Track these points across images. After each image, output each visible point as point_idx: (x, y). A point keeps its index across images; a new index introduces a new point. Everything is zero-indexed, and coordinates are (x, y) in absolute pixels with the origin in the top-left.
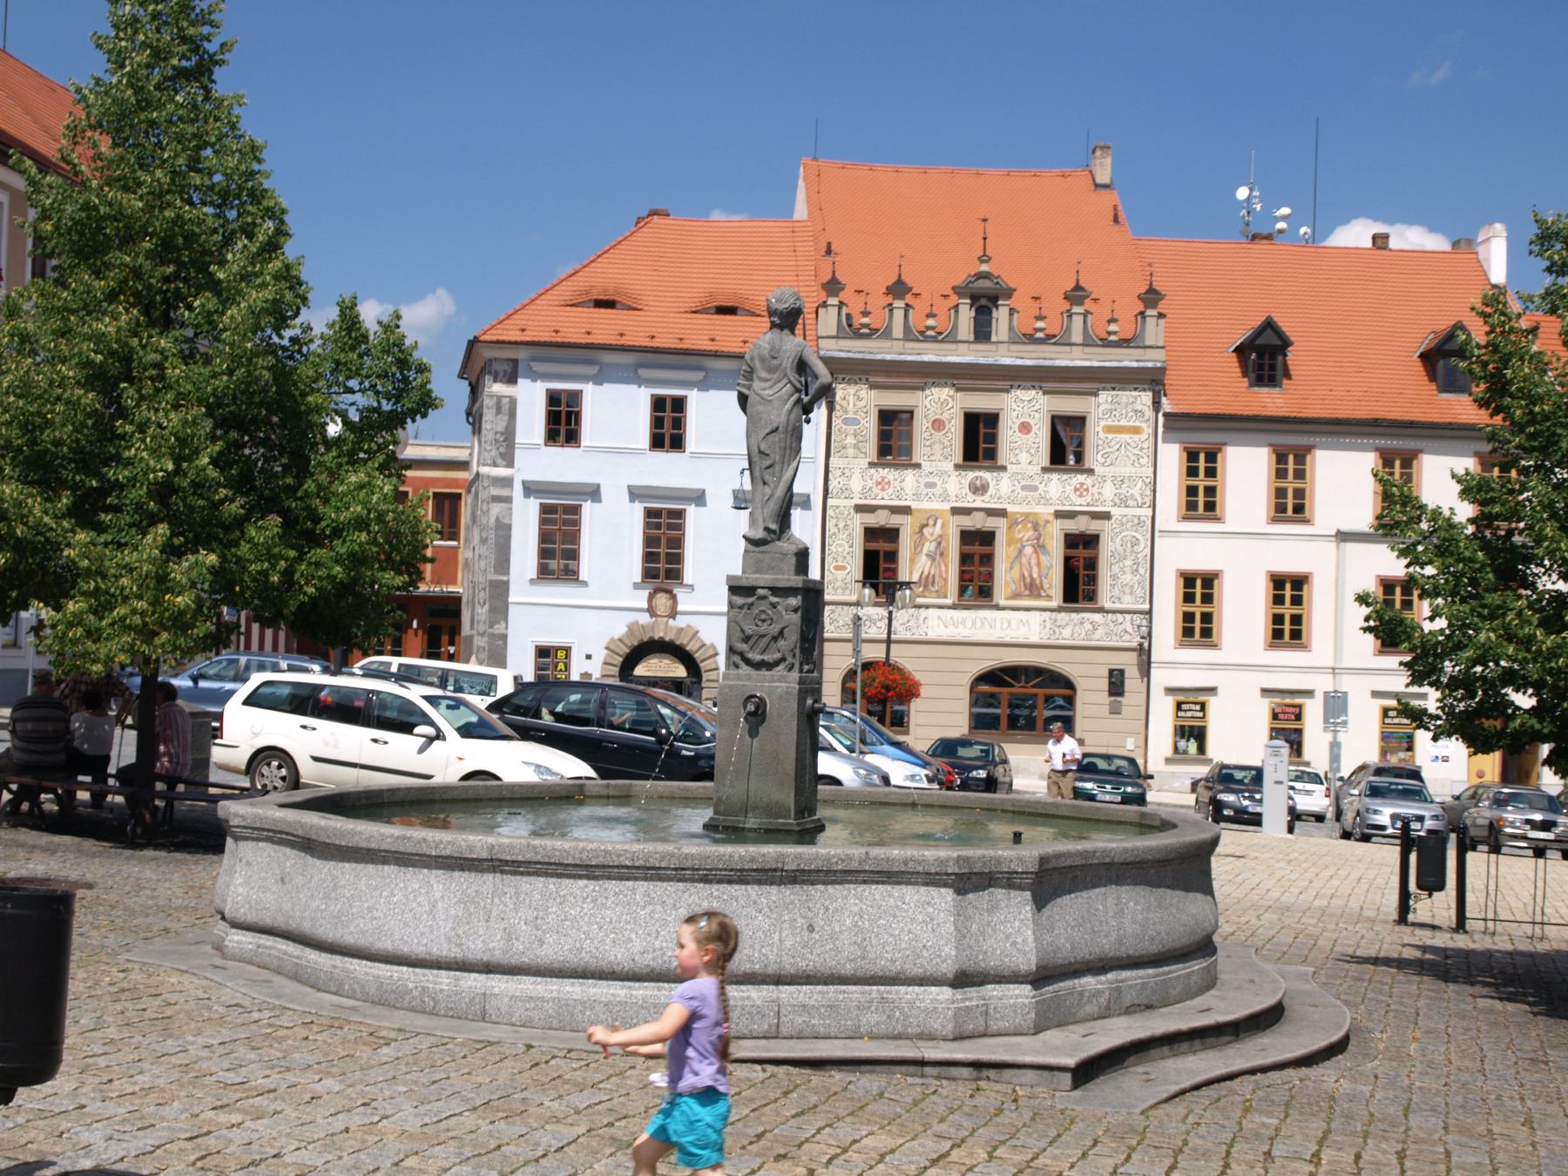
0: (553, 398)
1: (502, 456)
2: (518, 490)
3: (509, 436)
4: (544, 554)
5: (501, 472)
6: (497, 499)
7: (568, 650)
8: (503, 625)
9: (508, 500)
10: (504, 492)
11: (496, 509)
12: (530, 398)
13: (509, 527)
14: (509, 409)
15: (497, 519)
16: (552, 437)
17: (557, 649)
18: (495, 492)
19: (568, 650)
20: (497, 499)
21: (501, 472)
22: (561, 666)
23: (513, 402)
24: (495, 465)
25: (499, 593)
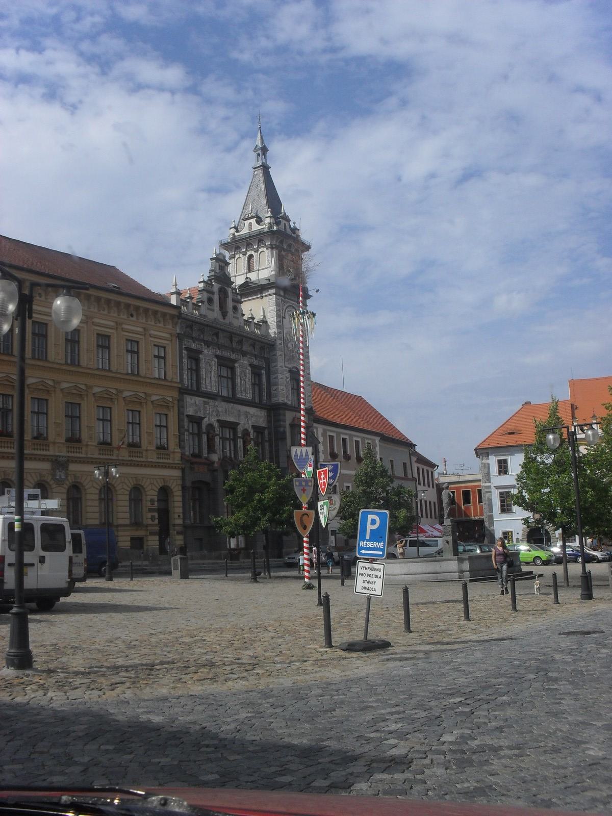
0: (499, 462)
1: (487, 480)
2: (493, 489)
3: (488, 474)
4: (502, 506)
5: (488, 484)
6: (487, 492)
7: (512, 532)
8: (493, 527)
9: (490, 492)
10: (489, 490)
11: (487, 495)
12: (493, 461)
13: (491, 500)
14: (488, 466)
15: (488, 498)
16: (500, 473)
17: (508, 532)
18: (487, 490)
19: (512, 532)
20: (487, 492)
21: (488, 484)
22: (510, 537)
23: (489, 464)
24: (486, 483)
25: (491, 517)
